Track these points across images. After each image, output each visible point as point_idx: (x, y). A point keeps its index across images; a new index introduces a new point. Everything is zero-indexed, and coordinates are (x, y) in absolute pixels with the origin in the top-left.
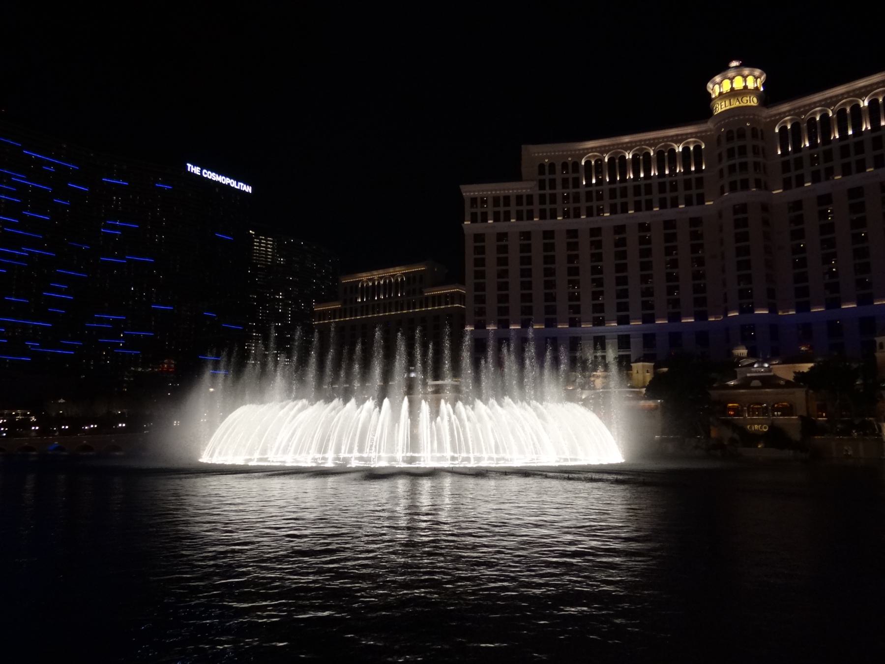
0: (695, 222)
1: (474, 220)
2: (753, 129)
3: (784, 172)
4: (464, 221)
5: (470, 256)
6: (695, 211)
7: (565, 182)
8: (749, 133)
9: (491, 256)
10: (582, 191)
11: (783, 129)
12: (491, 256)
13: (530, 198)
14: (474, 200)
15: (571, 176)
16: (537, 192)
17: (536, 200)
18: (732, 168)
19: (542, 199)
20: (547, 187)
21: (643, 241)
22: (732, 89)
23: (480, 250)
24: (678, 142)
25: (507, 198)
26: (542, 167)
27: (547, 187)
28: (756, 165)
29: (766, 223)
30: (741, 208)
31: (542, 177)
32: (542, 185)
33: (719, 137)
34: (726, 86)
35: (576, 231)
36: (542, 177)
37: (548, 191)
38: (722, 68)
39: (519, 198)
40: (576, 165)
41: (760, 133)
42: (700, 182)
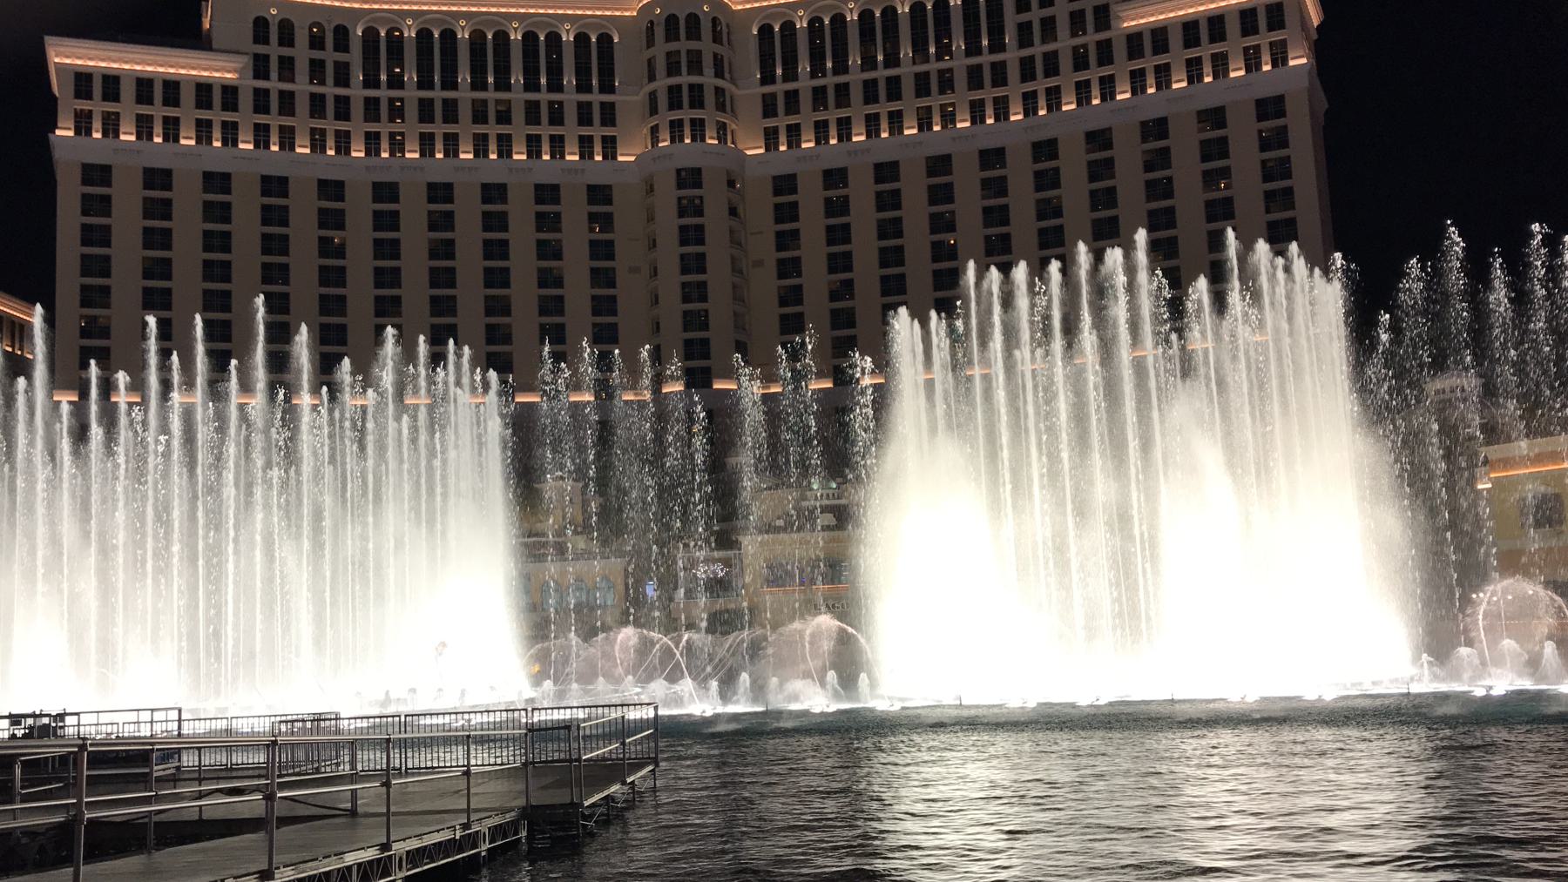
0: (599, 193)
1: (83, 124)
2: (715, 21)
4: (55, 127)
5: (69, 219)
7: (317, 68)
8: (706, 27)
9: (127, 221)
12: (127, 221)
13: (230, 94)
14: (82, 81)
15: (330, 56)
17: (246, 100)
18: (674, 91)
20: (274, 75)
23: (97, 205)
25: (172, 88)
26: (261, 25)
27: (274, 75)
28: (719, 91)
29: (733, 212)
30: (690, 178)
31: (261, 49)
32: (260, 68)
35: (340, 185)
36: (261, 49)
37: (274, 85)
39: (203, 91)
40: (342, 34)
41: (725, 30)
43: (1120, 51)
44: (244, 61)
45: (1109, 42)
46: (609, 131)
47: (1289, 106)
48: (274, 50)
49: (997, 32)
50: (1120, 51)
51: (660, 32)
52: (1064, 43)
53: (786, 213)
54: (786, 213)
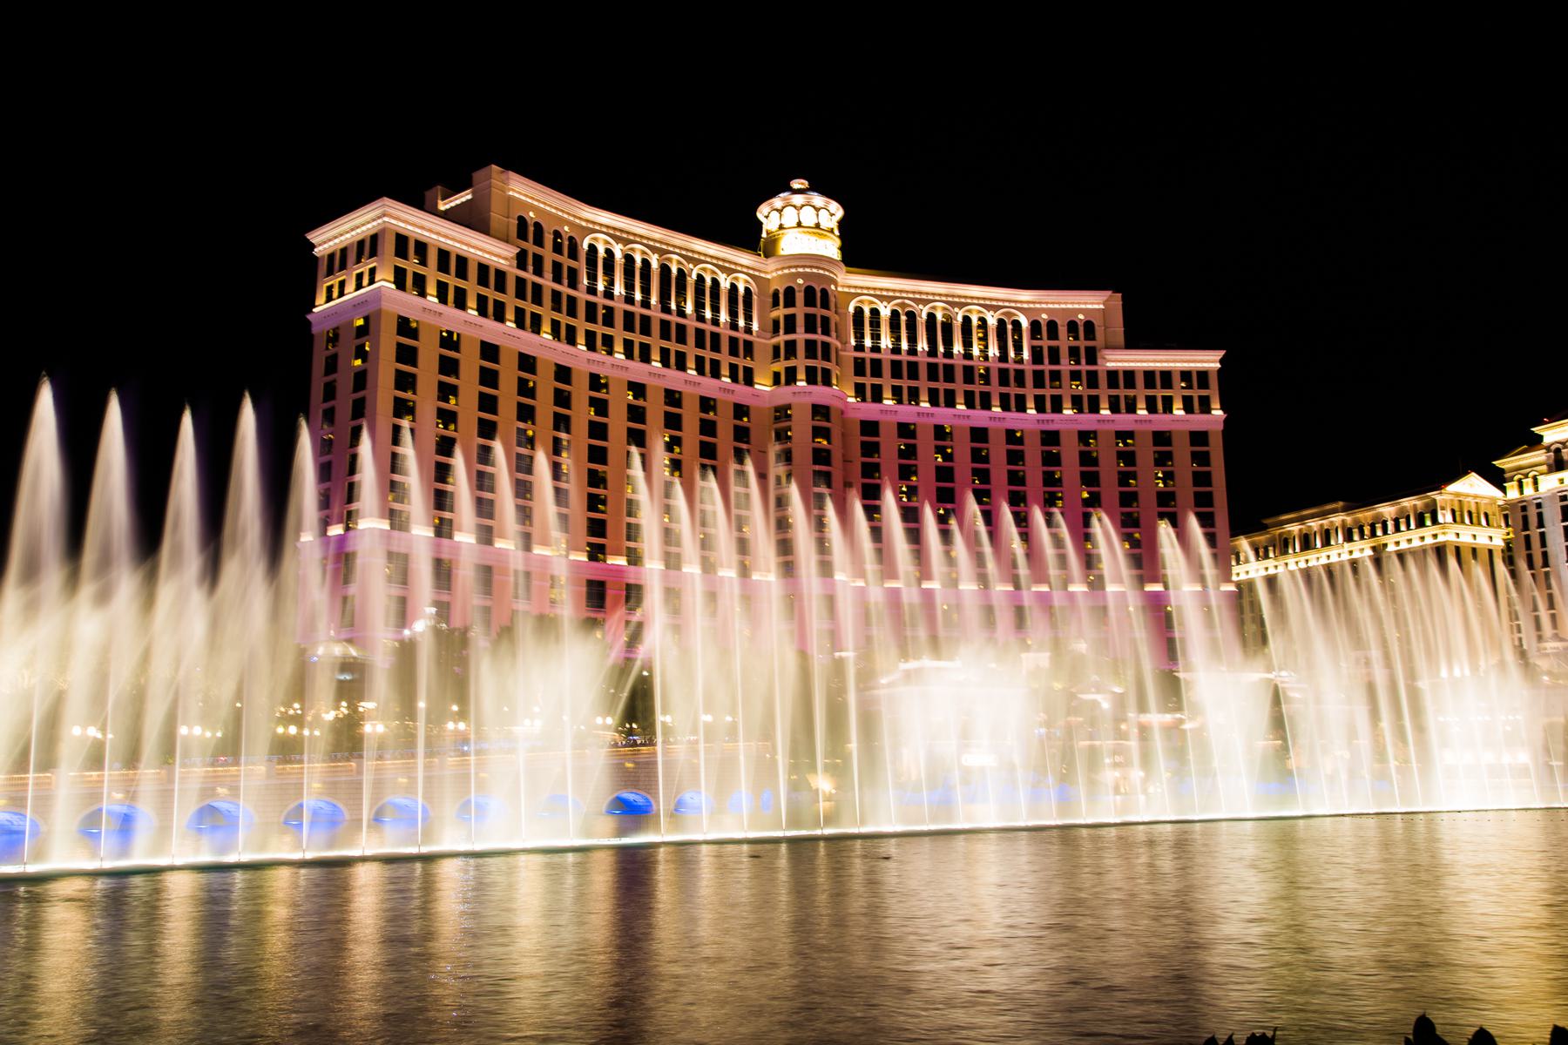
0: (740, 410)
3: (856, 374)
6: (741, 393)
8: (832, 299)
10: (582, 296)
11: (859, 312)
13: (501, 275)
16: (513, 271)
17: (511, 285)
19: (521, 282)
21: (977, 456)
22: (818, 226)
24: (729, 271)
25: (462, 262)
33: (790, 292)
34: (808, 217)
37: (529, 276)
38: (781, 186)
42: (749, 346)
43: (1103, 380)
44: (511, 251)
45: (1095, 372)
46: (748, 363)
47: (1212, 440)
48: (531, 248)
49: (1018, 348)
50: (1103, 380)
51: (800, 297)
52: (1066, 366)
53: (870, 449)
54: (870, 449)
